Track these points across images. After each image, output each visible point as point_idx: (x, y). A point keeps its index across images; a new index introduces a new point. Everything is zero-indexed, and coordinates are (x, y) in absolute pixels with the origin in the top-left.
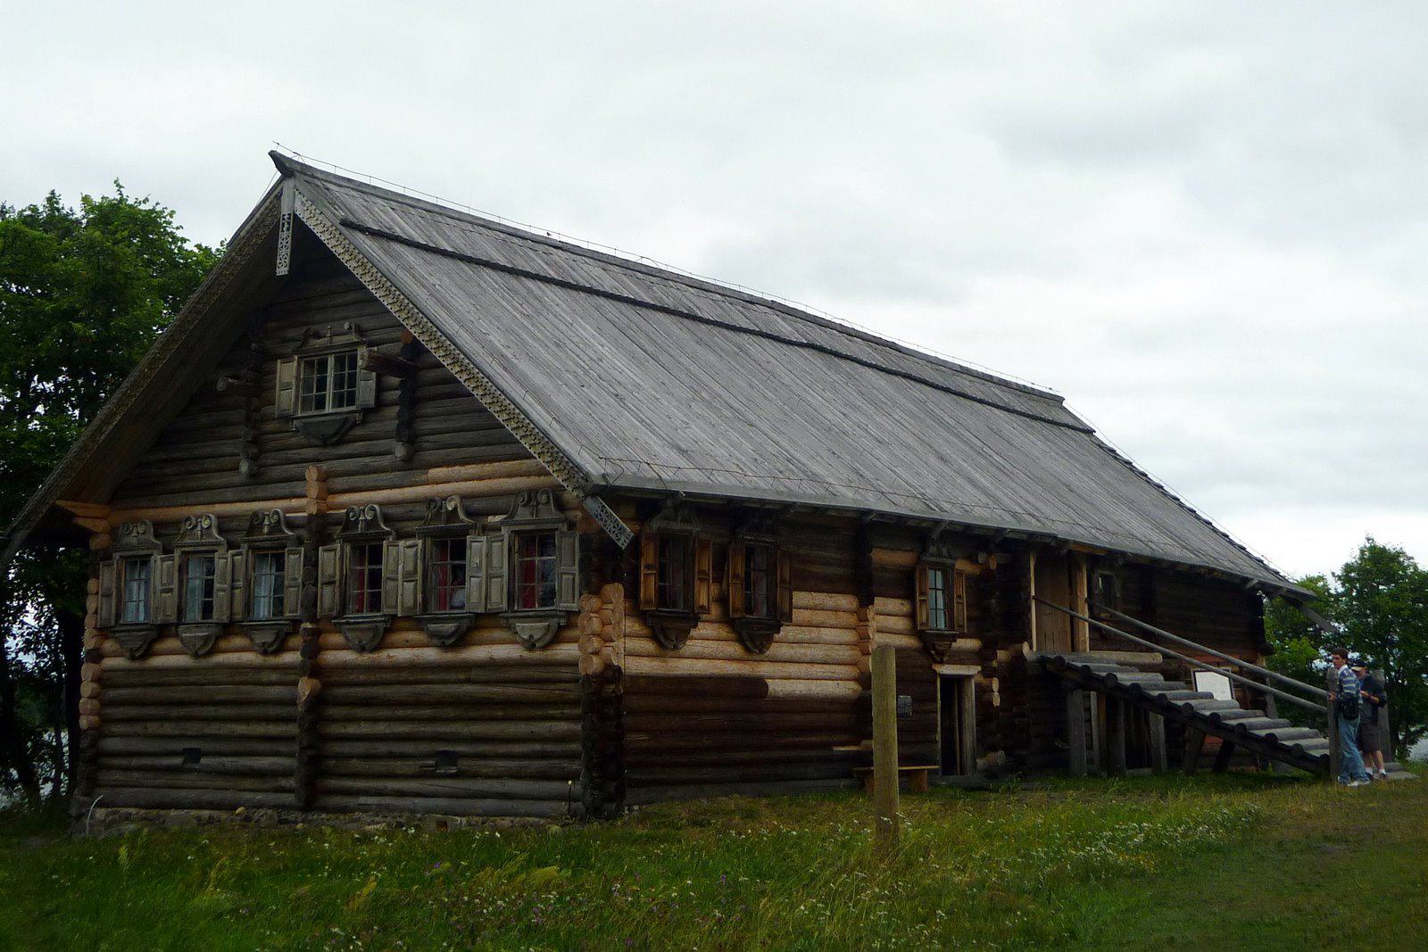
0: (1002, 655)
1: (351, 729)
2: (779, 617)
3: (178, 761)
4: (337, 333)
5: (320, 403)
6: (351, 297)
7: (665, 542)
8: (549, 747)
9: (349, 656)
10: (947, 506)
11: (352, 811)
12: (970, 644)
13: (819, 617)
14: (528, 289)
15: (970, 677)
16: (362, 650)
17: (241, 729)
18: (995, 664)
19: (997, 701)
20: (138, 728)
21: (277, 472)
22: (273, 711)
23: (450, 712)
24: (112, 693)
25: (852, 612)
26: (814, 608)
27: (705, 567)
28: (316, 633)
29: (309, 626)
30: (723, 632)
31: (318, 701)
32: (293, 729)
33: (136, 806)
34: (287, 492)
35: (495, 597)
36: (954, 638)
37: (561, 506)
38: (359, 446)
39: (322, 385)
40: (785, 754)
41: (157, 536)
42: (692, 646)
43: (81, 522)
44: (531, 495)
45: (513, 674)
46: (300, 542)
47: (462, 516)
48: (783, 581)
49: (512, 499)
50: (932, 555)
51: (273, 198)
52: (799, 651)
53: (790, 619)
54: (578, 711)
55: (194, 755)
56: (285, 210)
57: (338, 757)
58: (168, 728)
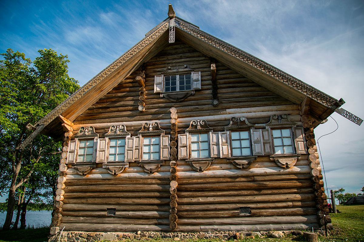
23: (245, 192)
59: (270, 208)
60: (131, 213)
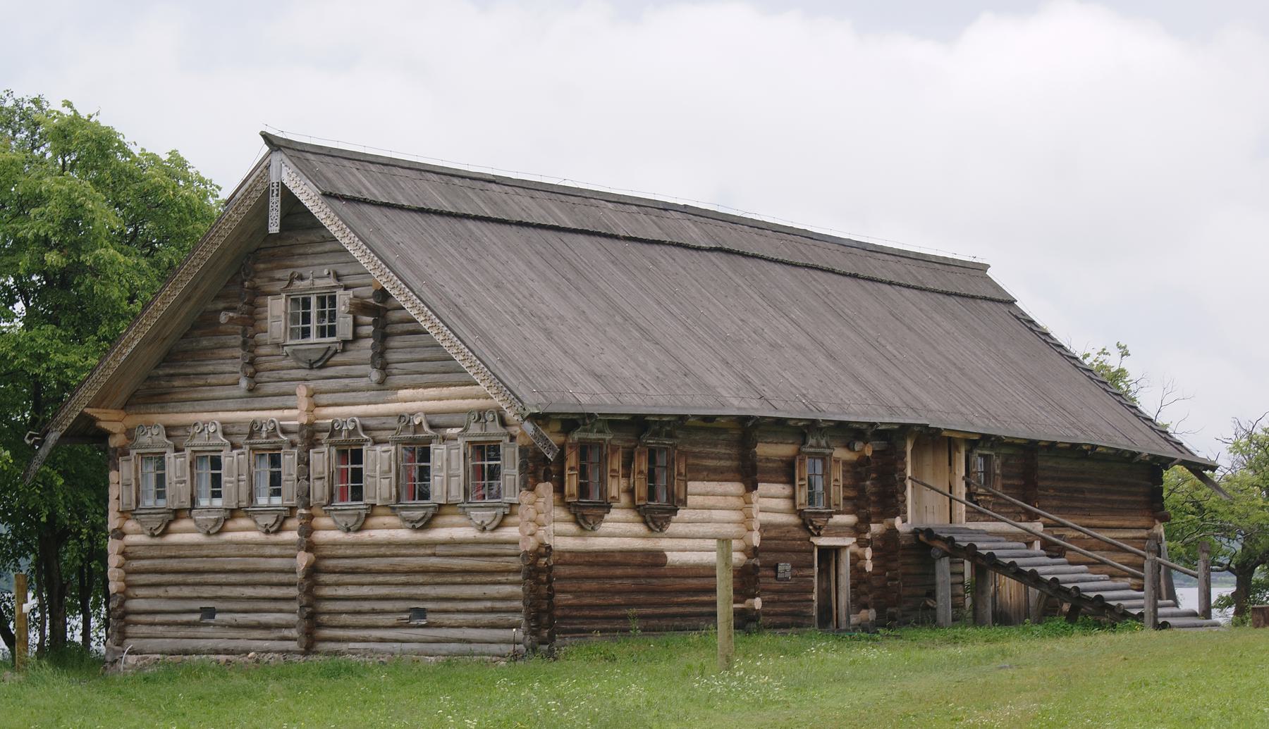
0: (876, 528)
1: (341, 592)
2: (677, 502)
3: (196, 617)
4: (316, 278)
5: (306, 333)
6: (328, 247)
7: (584, 449)
8: (498, 605)
9: (338, 535)
10: (824, 406)
11: (343, 654)
12: (849, 519)
13: (710, 501)
14: (470, 230)
15: (845, 547)
17: (249, 592)
18: (868, 536)
19: (869, 567)
20: (160, 592)
21: (270, 388)
22: (275, 578)
23: (420, 578)
24: (135, 564)
25: (739, 496)
26: (706, 494)
27: (616, 467)
28: (311, 517)
29: (304, 511)
30: (631, 515)
31: (313, 571)
32: (293, 592)
33: (162, 653)
34: (280, 404)
35: (454, 492)
36: (830, 515)
37: (504, 423)
38: (340, 370)
39: (306, 318)
40: (681, 610)
41: (168, 437)
42: (606, 527)
43: (103, 425)
44: (481, 415)
45: (468, 550)
46: (293, 445)
47: (426, 428)
48: (680, 474)
49: (466, 416)
50: (811, 446)
51: (263, 167)
52: (693, 529)
53: (685, 503)
54: (519, 578)
55: (210, 613)
56: (274, 179)
57: (330, 613)
58: (186, 591)
59: (458, 611)
60: (241, 618)
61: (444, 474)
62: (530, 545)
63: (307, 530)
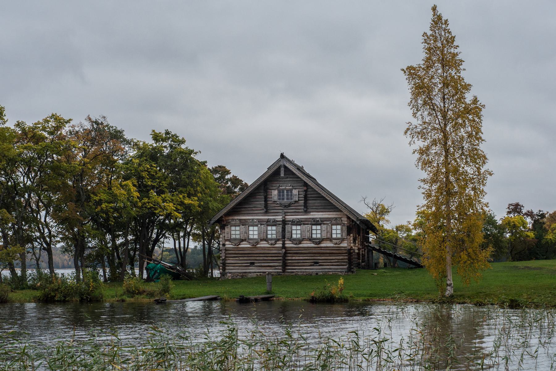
5: (283, 199)
16: (296, 244)
31: (286, 253)
32: (281, 258)
39: (283, 195)
55: (253, 263)
60: (262, 264)
61: (326, 231)
62: (350, 248)
63: (284, 244)
